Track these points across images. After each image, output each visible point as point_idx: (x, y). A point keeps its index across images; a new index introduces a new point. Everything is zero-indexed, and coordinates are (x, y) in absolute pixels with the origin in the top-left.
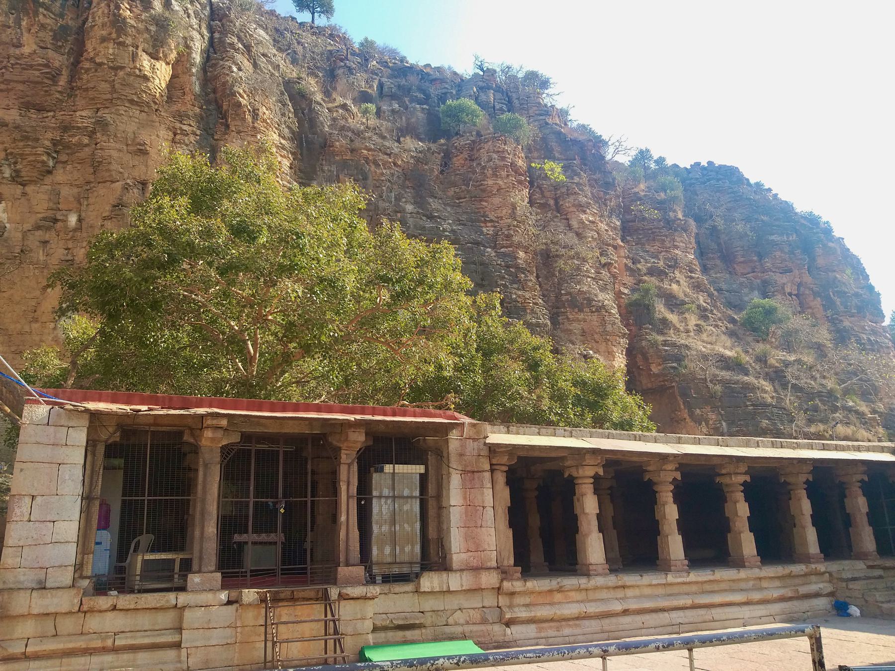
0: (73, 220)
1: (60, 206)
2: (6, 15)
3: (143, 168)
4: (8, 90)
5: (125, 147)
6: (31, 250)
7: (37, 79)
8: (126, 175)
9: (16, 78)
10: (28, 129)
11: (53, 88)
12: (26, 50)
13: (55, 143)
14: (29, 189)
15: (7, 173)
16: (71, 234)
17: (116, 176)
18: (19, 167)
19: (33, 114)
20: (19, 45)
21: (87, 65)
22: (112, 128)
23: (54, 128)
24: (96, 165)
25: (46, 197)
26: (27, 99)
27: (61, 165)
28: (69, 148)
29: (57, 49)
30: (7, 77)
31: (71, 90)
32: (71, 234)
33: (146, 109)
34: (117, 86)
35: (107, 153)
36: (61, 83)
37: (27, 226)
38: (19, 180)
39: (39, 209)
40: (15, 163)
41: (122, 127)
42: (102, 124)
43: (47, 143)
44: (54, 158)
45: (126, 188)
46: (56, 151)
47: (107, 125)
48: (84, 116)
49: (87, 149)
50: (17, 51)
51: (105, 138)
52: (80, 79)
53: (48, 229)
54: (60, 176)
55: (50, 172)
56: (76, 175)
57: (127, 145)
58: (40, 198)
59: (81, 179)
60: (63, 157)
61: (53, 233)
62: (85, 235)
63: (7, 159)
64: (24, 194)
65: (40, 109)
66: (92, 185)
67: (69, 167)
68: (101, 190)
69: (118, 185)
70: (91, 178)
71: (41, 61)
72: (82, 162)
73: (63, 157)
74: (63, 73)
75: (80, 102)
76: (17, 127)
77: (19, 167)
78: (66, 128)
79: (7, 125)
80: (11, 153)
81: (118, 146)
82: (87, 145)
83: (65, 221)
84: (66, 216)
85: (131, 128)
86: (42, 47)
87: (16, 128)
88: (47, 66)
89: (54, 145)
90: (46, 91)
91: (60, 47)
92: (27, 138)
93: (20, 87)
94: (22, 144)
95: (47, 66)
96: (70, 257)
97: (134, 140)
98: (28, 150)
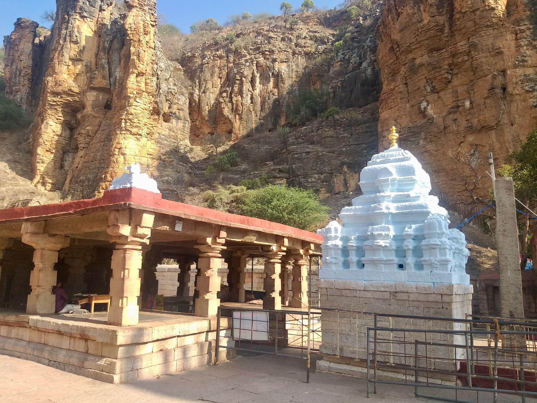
0: (467, 104)
1: (459, 98)
2: (413, 8)
3: (502, 62)
4: (421, 46)
5: (489, 54)
6: (449, 126)
7: (433, 35)
8: (492, 70)
9: (423, 39)
11: (442, 36)
12: (425, 22)
13: (450, 65)
14: (441, 94)
15: (429, 89)
16: (468, 112)
18: (434, 84)
19: (435, 54)
20: (422, 20)
21: (458, 16)
22: (479, 46)
23: (448, 58)
24: (474, 70)
25: (450, 96)
26: (431, 47)
27: (455, 76)
28: (457, 65)
29: (440, 14)
30: (419, 40)
31: (452, 34)
32: (468, 112)
33: (496, 27)
34: (477, 21)
35: (479, 61)
36: (446, 31)
37: (444, 114)
38: (435, 91)
39: (447, 103)
40: (432, 83)
41: (484, 43)
42: (474, 46)
43: (446, 67)
44: (451, 73)
45: (494, 77)
46: (451, 70)
47: (476, 45)
48: (462, 45)
49: (467, 63)
50: (422, 25)
51: (477, 53)
52: (455, 25)
53: (455, 112)
54: (455, 82)
55: (450, 82)
57: (490, 52)
58: (447, 97)
59: (467, 80)
60: (455, 71)
61: (458, 114)
62: (475, 110)
63: (427, 82)
64: (439, 97)
65: (438, 50)
69: (489, 77)
71: (433, 24)
72: (466, 70)
74: (446, 25)
75: (458, 37)
76: (429, 64)
77: (434, 84)
78: (454, 55)
79: (424, 65)
80: (429, 79)
81: (484, 55)
82: (467, 61)
83: (464, 106)
84: (464, 103)
85: (490, 42)
86: (433, 17)
87: (428, 65)
88: (437, 25)
89: (450, 66)
90: (439, 39)
91: (441, 12)
92: (435, 68)
93: (426, 42)
95: (437, 25)
96: (470, 125)
97: (493, 48)
98: (437, 74)
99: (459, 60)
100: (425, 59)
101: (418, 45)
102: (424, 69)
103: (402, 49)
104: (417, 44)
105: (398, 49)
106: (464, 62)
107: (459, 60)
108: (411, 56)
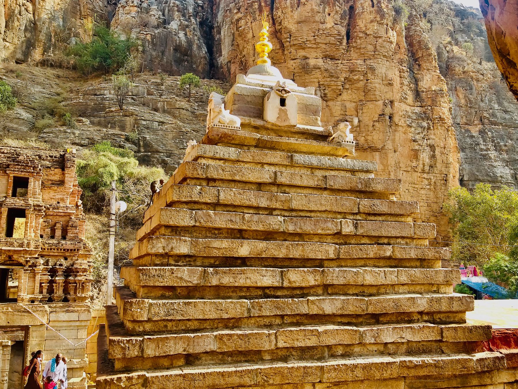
10: (333, 72)
17: (378, 98)
24: (366, 91)
27: (345, 90)
49: (361, 82)
56: (354, 96)
59: (357, 98)
66: (364, 102)
67: (349, 91)
68: (370, 105)
70: (363, 98)
72: (358, 89)
73: (347, 86)
79: (320, 69)
94: (329, 79)
99: (355, 78)
100: (320, 62)
101: (315, 46)
102: (320, 73)
103: (295, 42)
104: (315, 44)
105: (288, 40)
106: (359, 80)
107: (355, 78)
108: (302, 53)
